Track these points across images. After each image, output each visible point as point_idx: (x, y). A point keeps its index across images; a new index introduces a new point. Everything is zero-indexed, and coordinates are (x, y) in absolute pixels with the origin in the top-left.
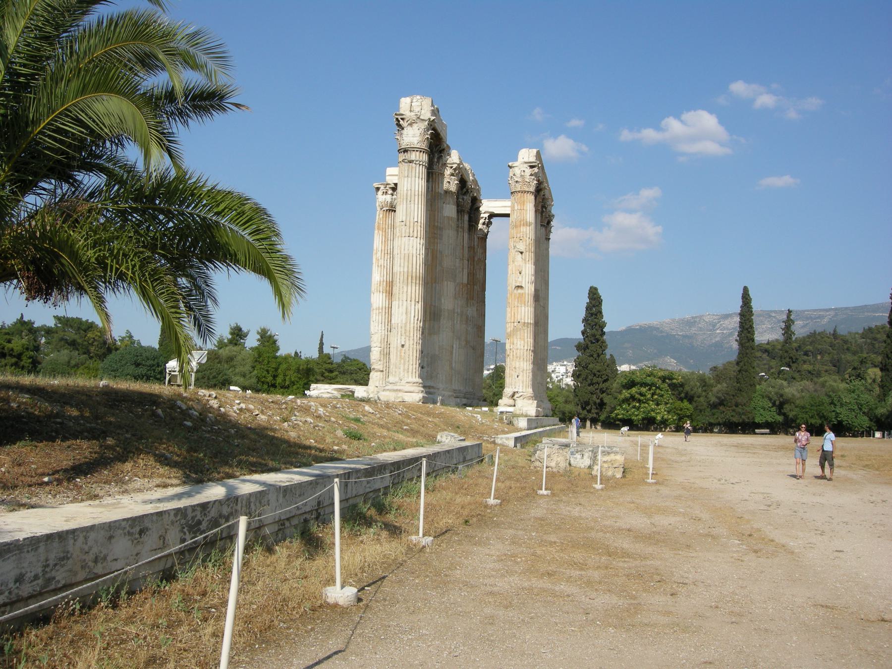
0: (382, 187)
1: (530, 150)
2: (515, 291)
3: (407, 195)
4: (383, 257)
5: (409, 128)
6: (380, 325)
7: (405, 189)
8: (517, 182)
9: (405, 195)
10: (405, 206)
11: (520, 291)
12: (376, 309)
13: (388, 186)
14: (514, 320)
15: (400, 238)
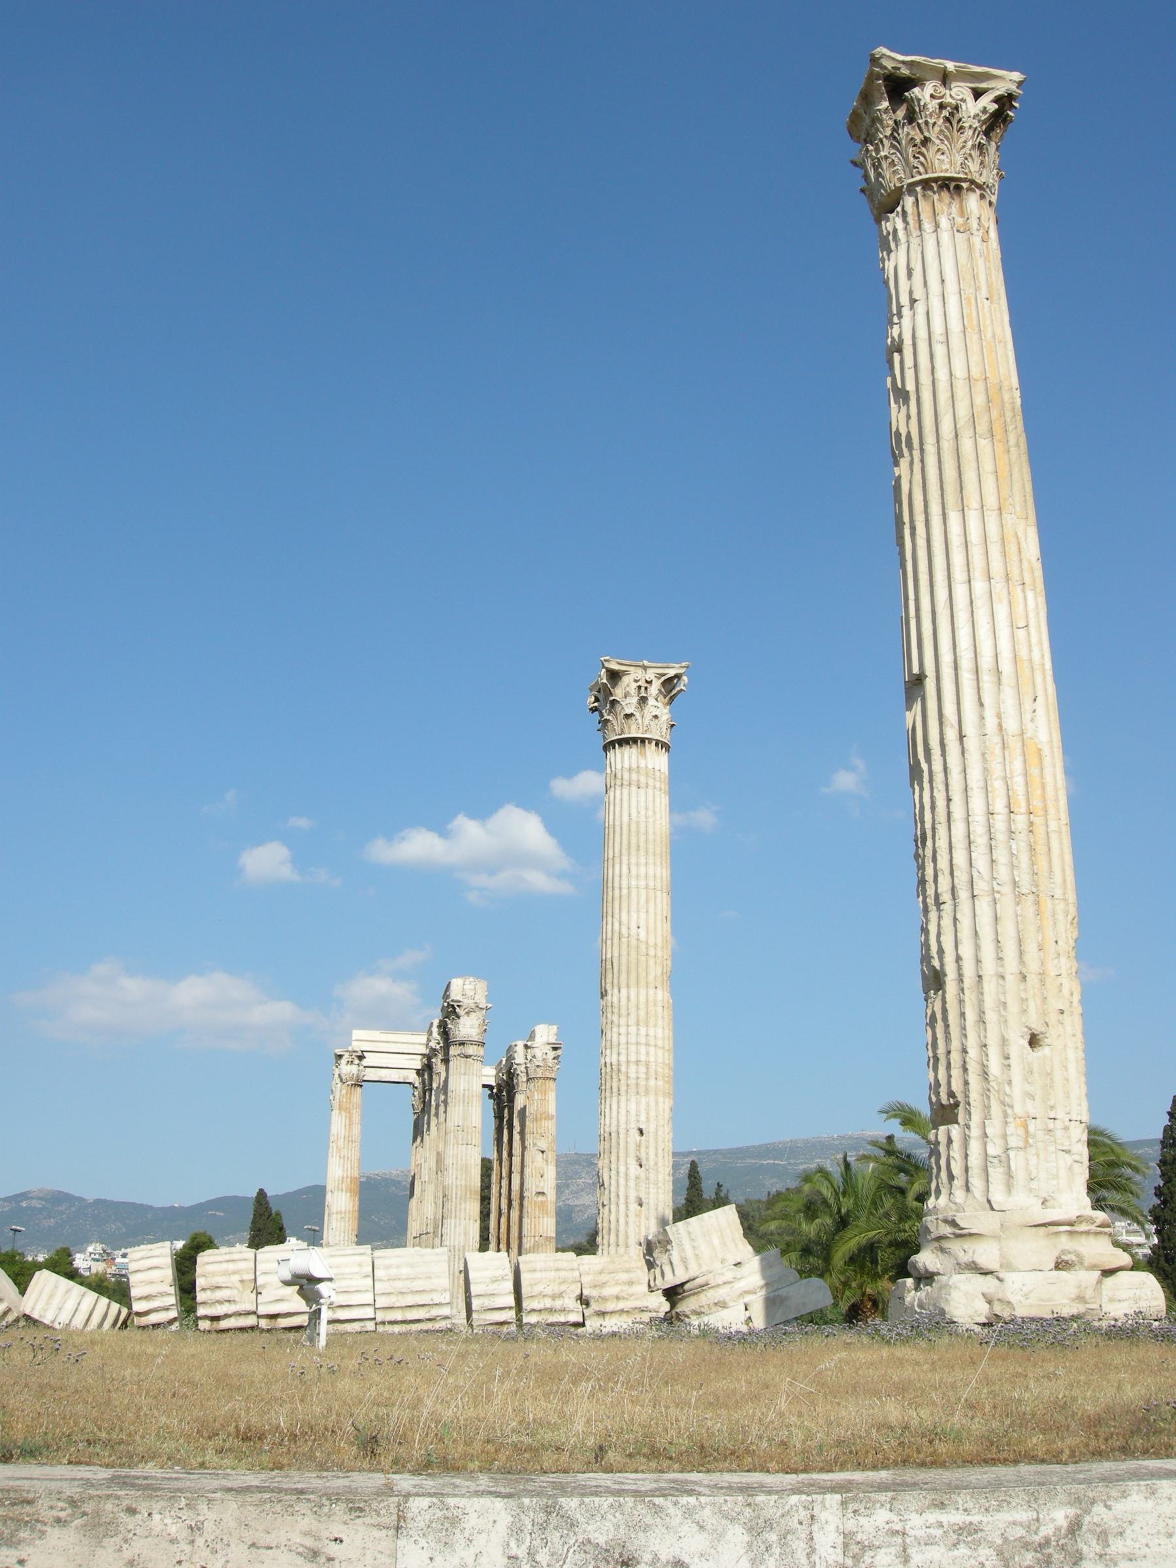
0: (347, 1055)
1: (550, 1027)
2: (535, 1199)
3: (464, 1095)
4: (346, 1146)
5: (466, 1017)
6: (342, 1234)
7: (462, 1089)
8: (538, 1066)
9: (461, 1095)
10: (461, 1107)
11: (541, 1198)
12: (337, 1213)
13: (354, 1054)
14: (535, 1233)
15: (456, 1146)
